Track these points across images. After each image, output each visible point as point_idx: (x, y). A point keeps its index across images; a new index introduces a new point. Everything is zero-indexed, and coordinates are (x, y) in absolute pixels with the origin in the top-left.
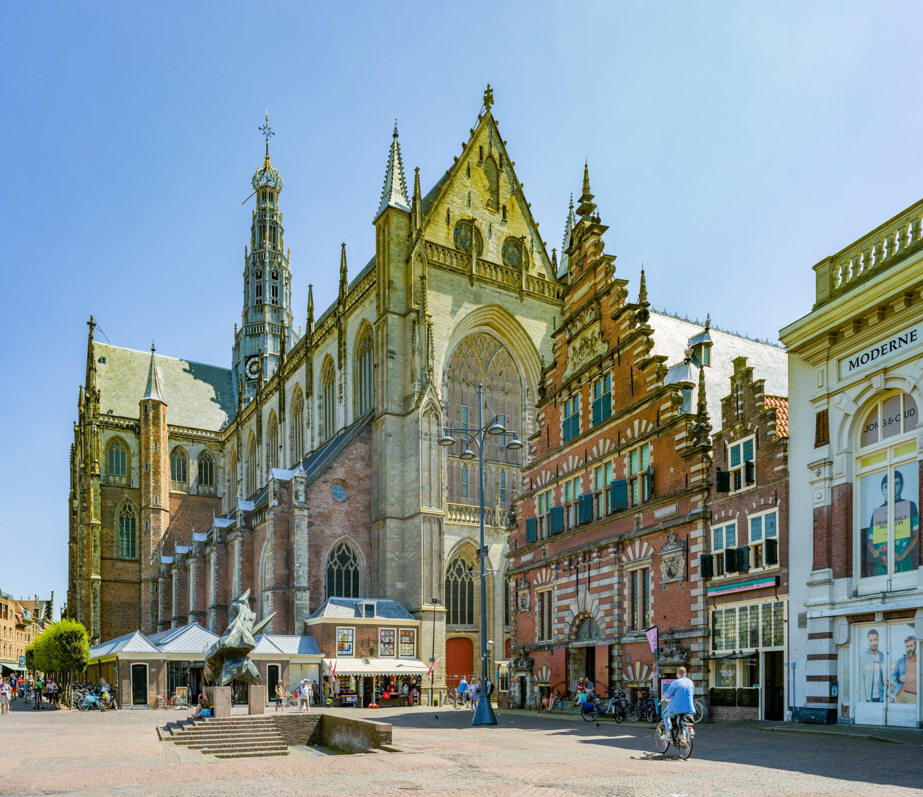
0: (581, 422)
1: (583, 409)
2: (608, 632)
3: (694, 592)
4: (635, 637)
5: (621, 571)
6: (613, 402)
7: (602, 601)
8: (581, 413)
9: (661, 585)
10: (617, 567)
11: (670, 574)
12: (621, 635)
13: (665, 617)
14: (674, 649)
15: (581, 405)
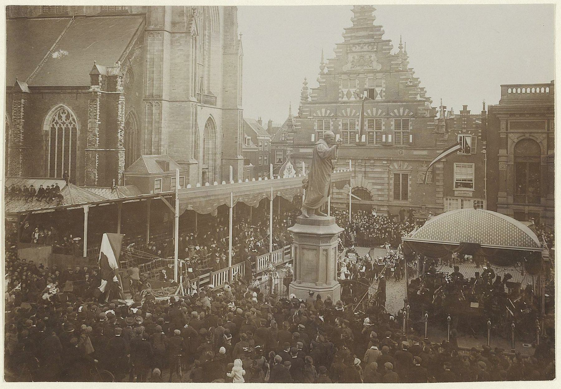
2: (380, 199)
3: (438, 190)
7: (374, 184)
10: (387, 170)
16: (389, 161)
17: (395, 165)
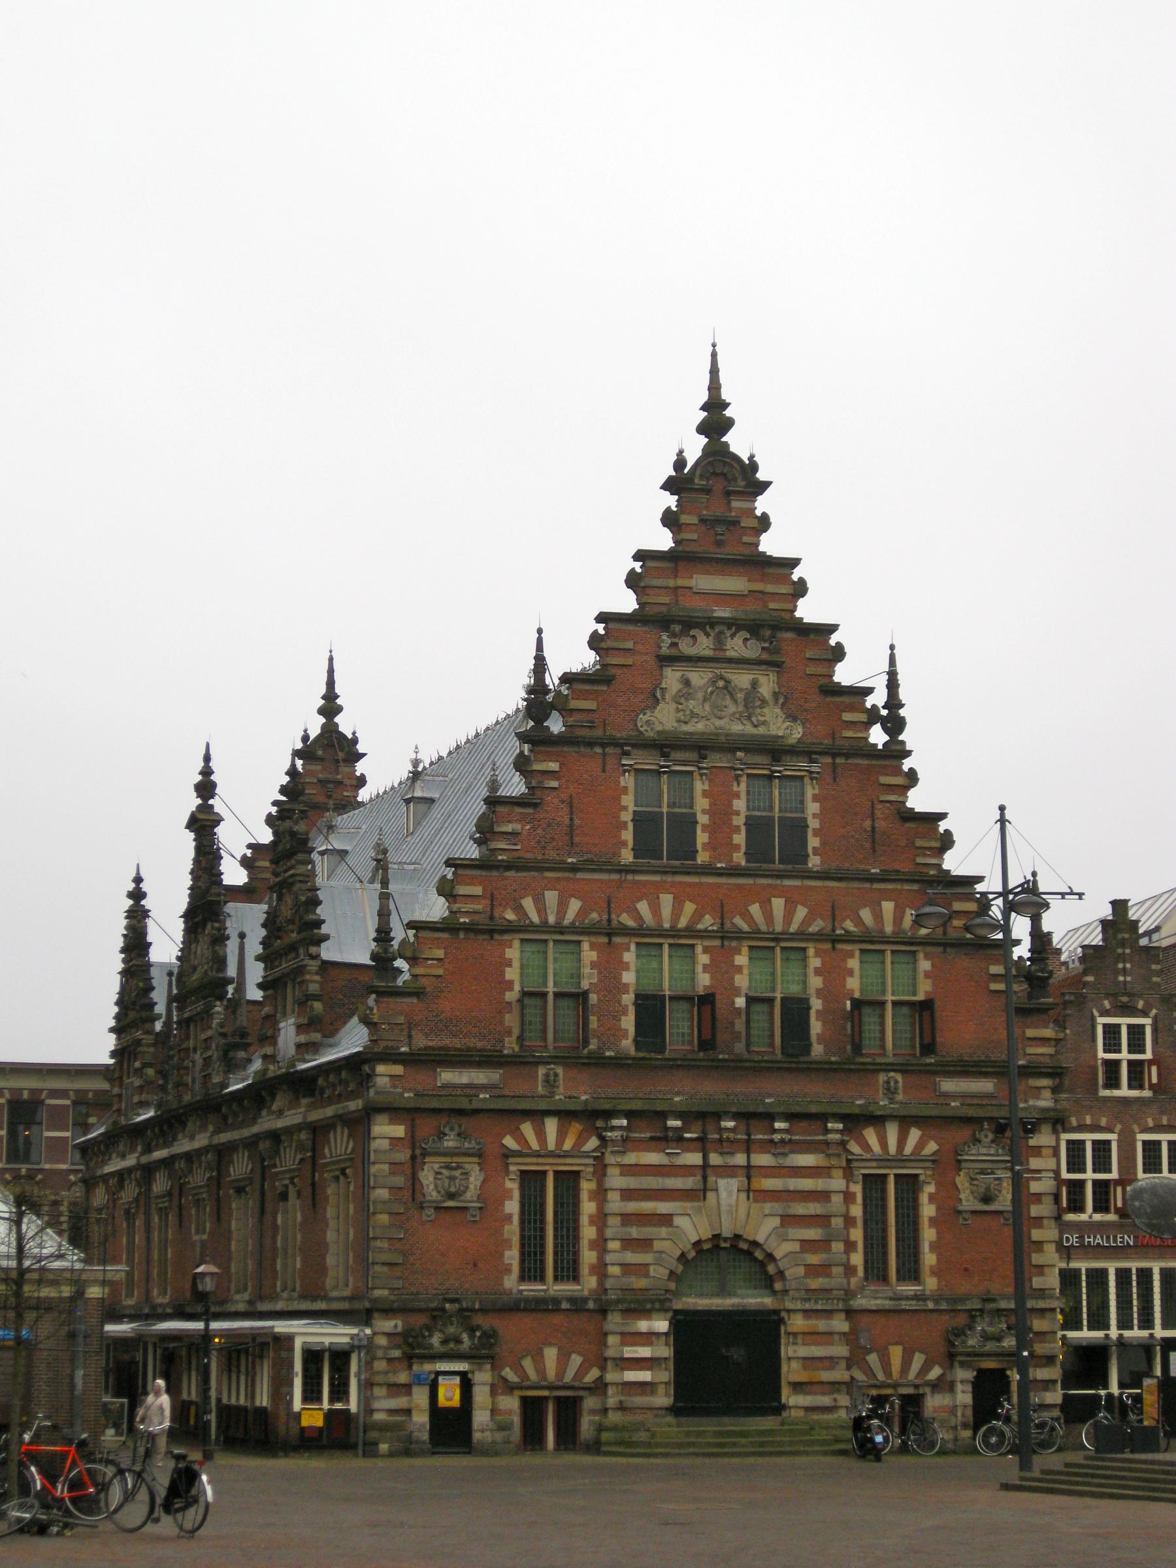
0: (702, 838)
1: (711, 812)
2: (816, 1283)
3: (1036, 1234)
4: (891, 1299)
5: (848, 1173)
6: (813, 842)
7: (788, 1220)
8: (703, 819)
9: (960, 1212)
10: (844, 1164)
11: (987, 1199)
12: (849, 1294)
13: (966, 1270)
14: (1004, 1326)
15: (701, 804)
16: (855, 1121)
17: (871, 1135)
